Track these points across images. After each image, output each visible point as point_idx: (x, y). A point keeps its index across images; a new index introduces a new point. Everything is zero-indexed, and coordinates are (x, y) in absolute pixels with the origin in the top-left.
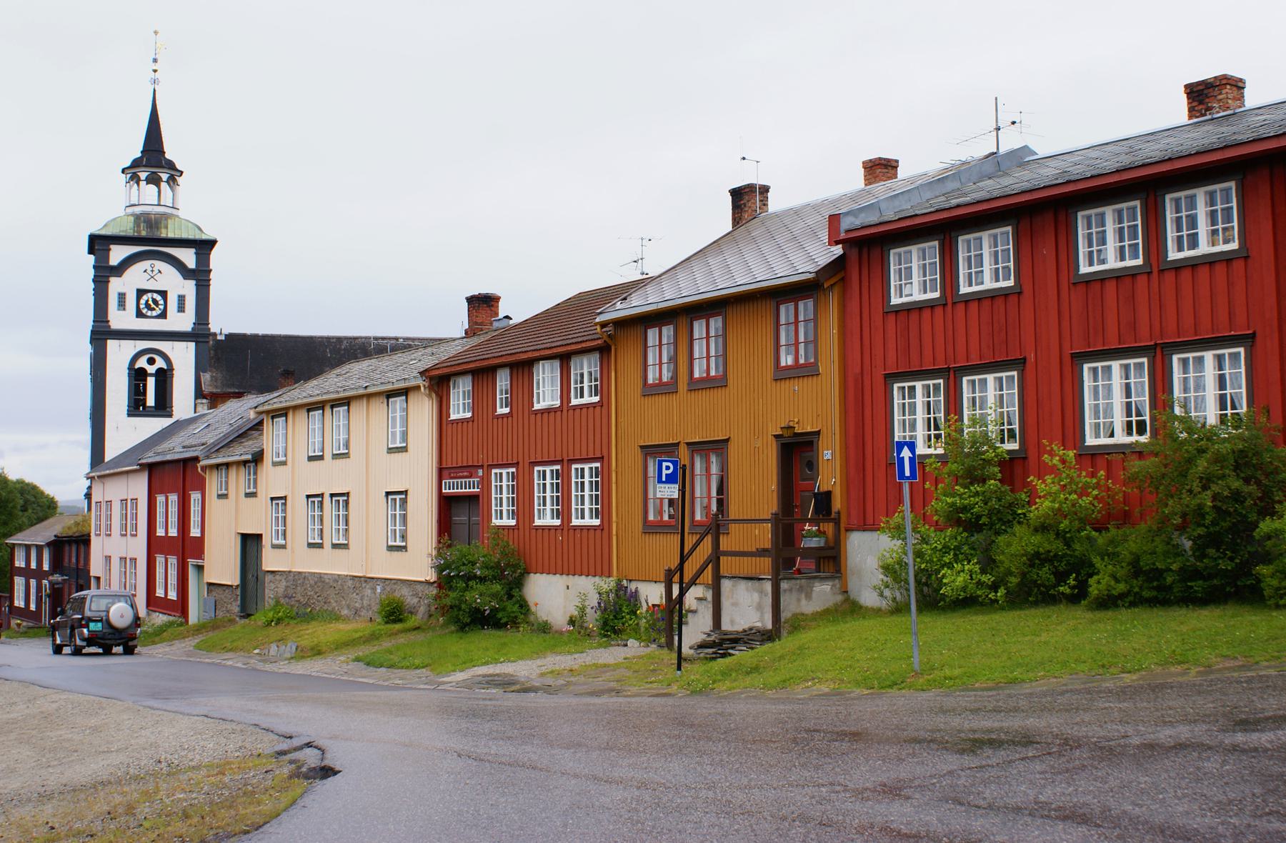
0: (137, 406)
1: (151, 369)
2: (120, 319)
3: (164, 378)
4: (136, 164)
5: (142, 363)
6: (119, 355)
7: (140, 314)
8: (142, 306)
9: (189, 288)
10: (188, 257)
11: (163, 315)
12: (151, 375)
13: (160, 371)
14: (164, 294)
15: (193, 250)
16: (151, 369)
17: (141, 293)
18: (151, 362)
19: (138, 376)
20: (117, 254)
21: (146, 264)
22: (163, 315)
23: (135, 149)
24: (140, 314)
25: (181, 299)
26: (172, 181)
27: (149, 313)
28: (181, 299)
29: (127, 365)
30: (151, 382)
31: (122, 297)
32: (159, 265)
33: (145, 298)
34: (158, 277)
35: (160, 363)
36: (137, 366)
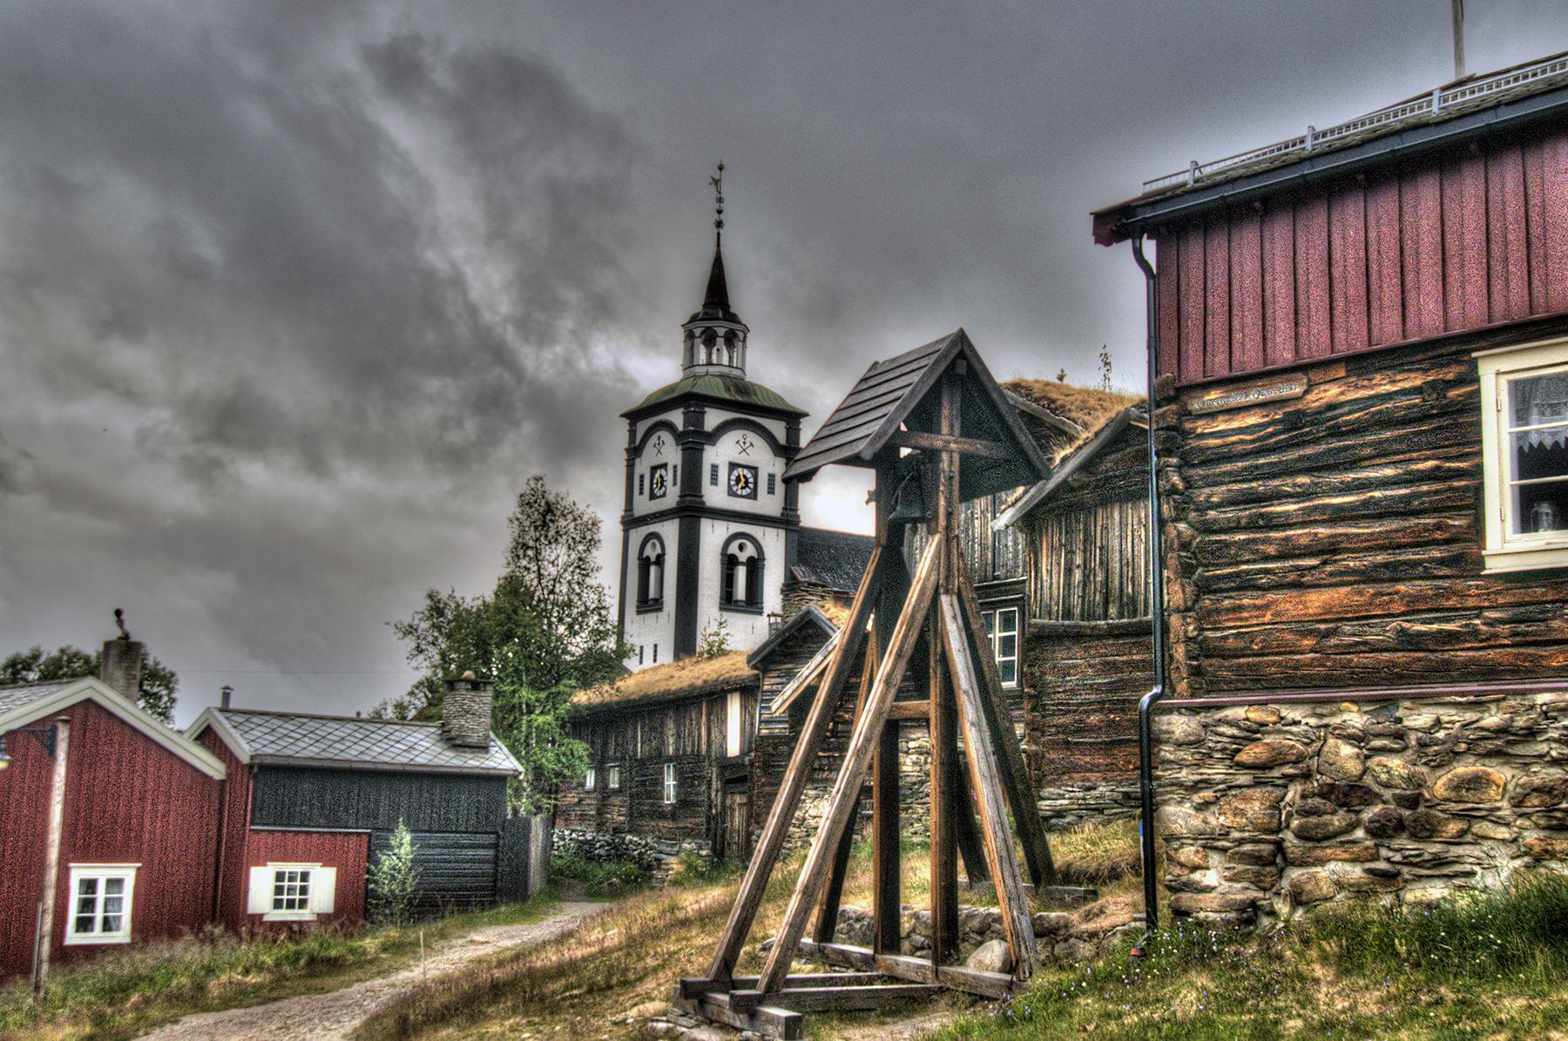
0: (727, 601)
1: (743, 557)
2: (715, 496)
4: (694, 319)
5: (733, 548)
6: (713, 536)
7: (732, 493)
10: (778, 429)
11: (753, 496)
13: (751, 559)
15: (783, 424)
16: (743, 557)
17: (733, 466)
18: (741, 547)
19: (729, 562)
20: (713, 418)
22: (753, 496)
23: (696, 304)
24: (732, 493)
26: (731, 339)
30: (741, 574)
31: (715, 468)
32: (752, 437)
33: (735, 473)
35: (750, 550)
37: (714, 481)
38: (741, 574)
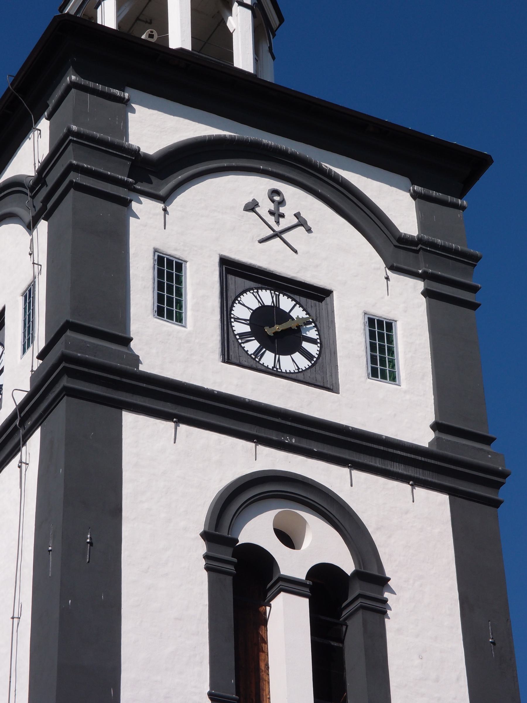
1: (294, 564)
3: (346, 604)
5: (258, 530)
8: (240, 328)
9: (406, 303)
12: (292, 586)
14: (315, 295)
16: (294, 564)
19: (242, 583)
21: (256, 186)
25: (380, 334)
27: (268, 359)
28: (380, 334)
29: (199, 520)
31: (169, 273)
34: (296, 237)
36: (245, 536)
37: (169, 305)
38: (288, 623)
